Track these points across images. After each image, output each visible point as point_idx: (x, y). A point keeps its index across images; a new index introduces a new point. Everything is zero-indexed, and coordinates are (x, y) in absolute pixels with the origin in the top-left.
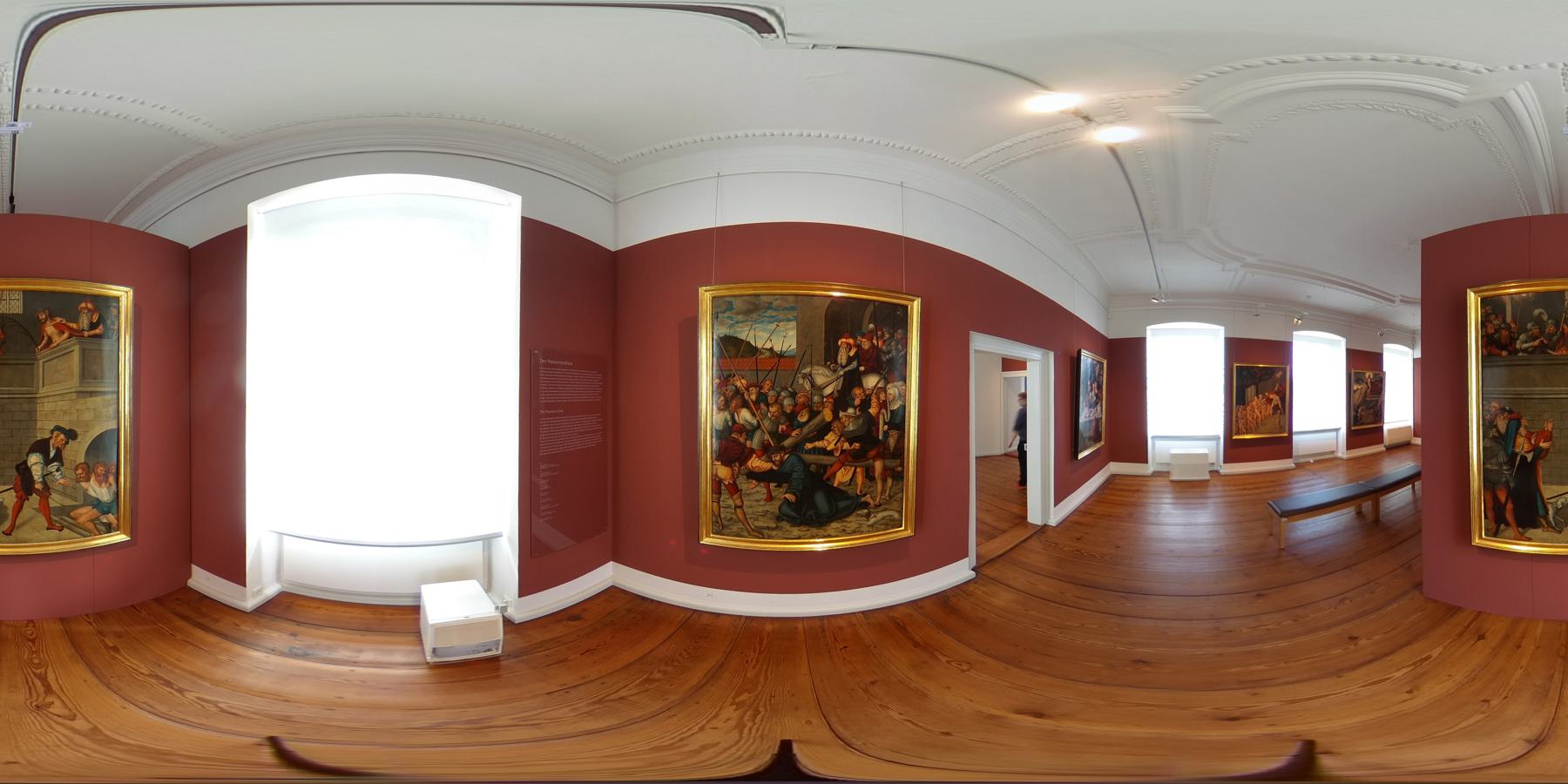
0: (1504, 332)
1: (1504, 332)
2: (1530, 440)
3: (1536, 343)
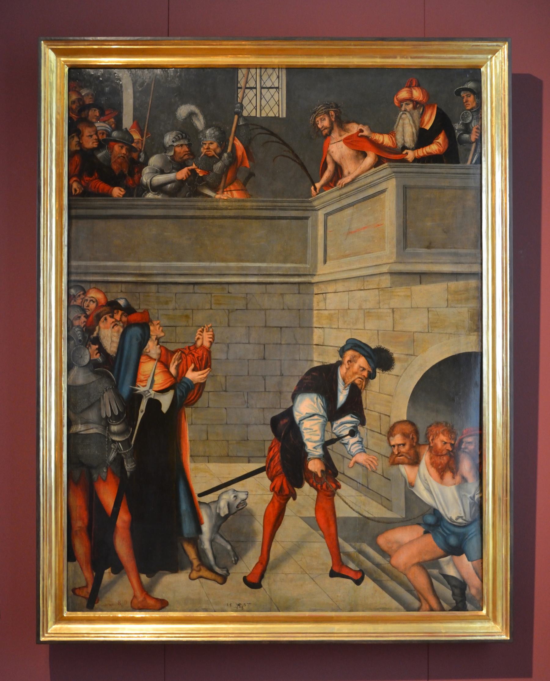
0: (117, 147)
1: (117, 147)
2: (167, 366)
3: (182, 174)
